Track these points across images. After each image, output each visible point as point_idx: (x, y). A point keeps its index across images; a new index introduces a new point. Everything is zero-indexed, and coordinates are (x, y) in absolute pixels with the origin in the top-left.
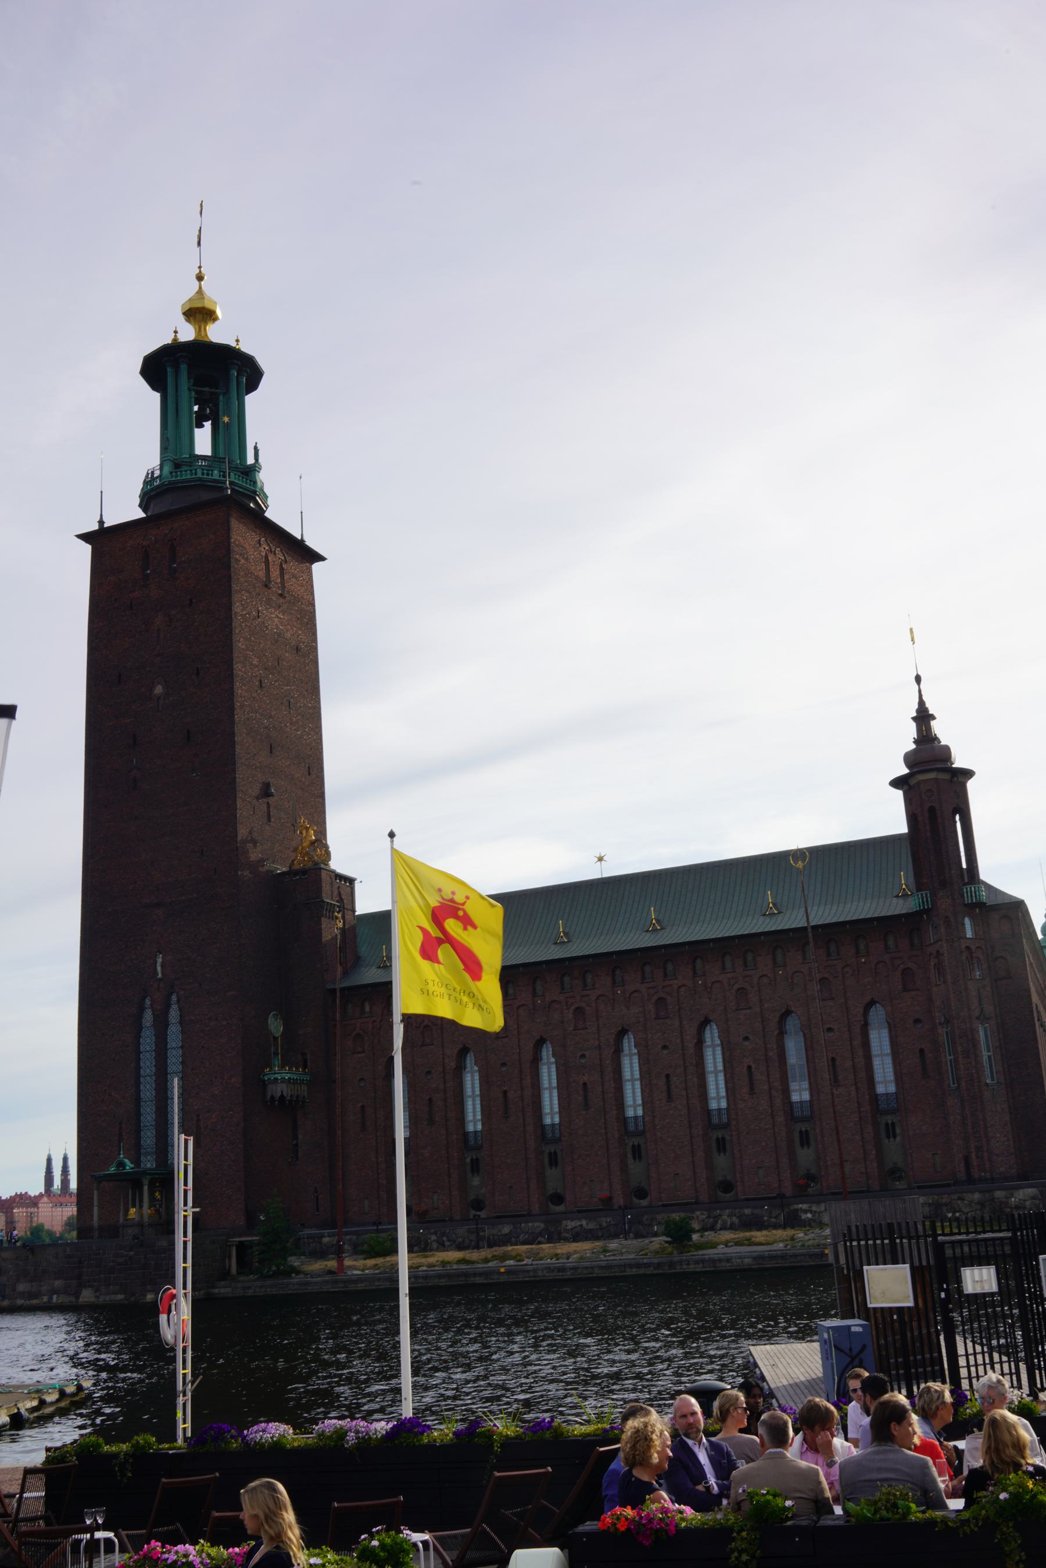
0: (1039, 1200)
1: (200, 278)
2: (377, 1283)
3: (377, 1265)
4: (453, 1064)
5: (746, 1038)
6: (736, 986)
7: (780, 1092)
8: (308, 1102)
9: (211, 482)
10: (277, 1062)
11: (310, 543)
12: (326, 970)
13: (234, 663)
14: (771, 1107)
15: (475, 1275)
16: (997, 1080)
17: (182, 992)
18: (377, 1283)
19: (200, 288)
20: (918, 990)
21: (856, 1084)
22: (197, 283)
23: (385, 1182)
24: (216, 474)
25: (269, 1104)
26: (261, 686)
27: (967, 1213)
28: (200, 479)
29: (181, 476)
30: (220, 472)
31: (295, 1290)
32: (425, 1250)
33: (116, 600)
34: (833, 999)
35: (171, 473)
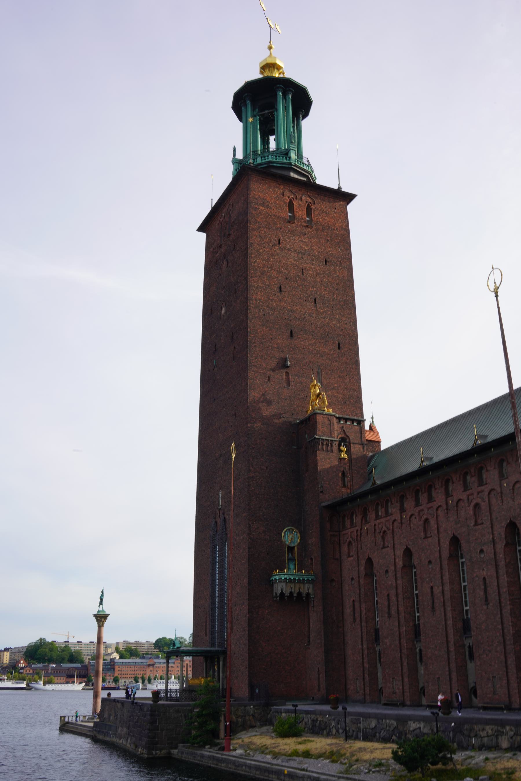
1: (270, 48)
8: (314, 598)
12: (322, 492)
13: (249, 277)
22: (268, 51)
26: (280, 290)
30: (262, 158)
31: (199, 760)
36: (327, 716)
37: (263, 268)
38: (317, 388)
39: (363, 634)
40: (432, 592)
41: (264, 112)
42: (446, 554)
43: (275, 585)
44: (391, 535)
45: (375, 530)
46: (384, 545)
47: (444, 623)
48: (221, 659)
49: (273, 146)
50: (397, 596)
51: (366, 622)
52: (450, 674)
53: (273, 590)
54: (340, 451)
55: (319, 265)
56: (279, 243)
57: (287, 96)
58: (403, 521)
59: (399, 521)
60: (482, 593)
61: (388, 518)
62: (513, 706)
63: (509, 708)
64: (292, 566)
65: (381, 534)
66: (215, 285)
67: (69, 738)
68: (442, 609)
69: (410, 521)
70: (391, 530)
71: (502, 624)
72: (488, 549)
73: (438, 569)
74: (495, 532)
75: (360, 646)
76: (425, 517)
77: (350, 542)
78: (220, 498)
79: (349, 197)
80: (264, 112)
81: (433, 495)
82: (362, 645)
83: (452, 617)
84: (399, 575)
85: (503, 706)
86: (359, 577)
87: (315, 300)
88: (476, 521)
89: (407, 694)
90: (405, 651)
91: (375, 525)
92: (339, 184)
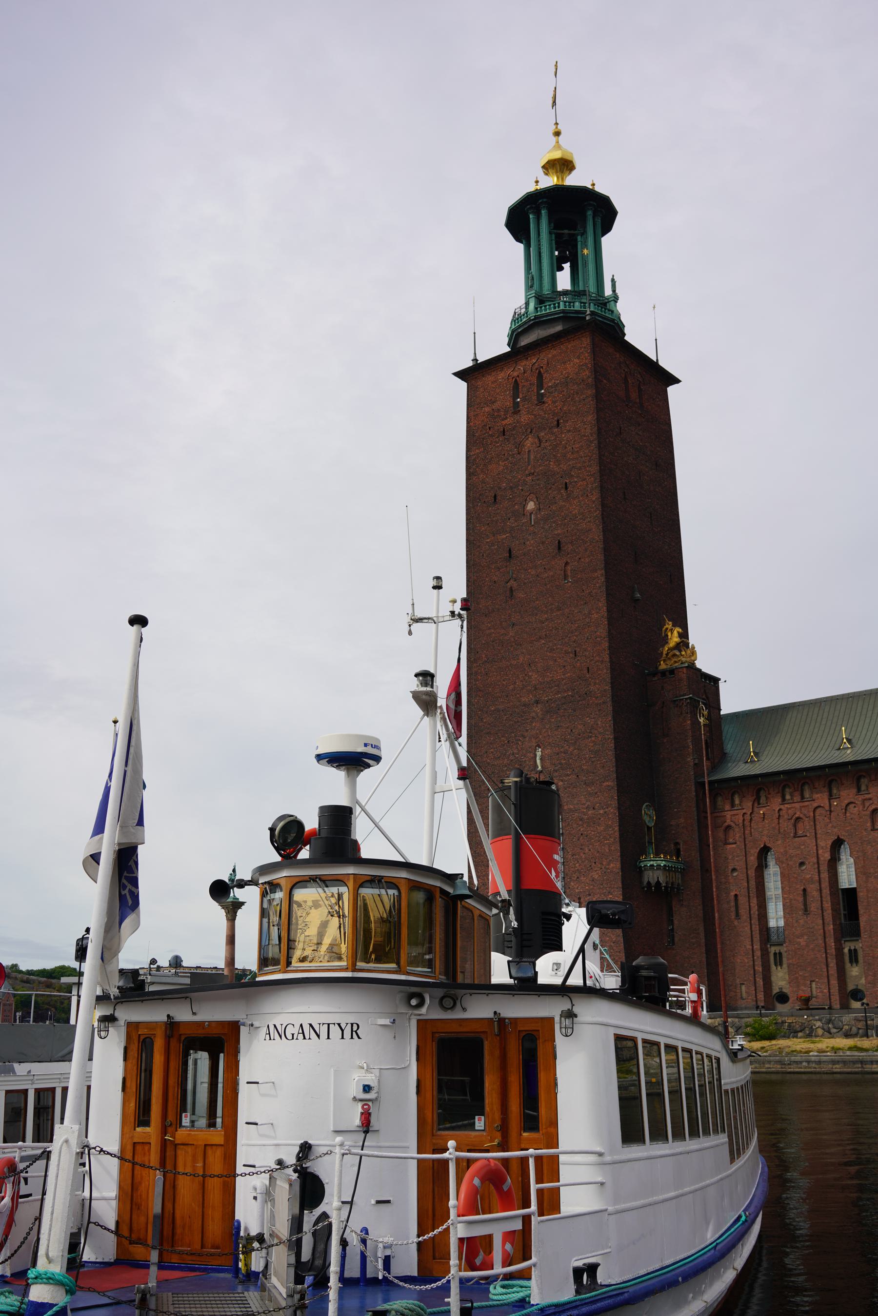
1: (557, 134)
2: (767, 1066)
3: (764, 1047)
4: (827, 856)
8: (682, 890)
9: (572, 313)
10: (651, 850)
15: (872, 1062)
17: (560, 783)
18: (767, 1066)
22: (554, 139)
23: (760, 969)
24: (577, 306)
25: (646, 889)
28: (563, 311)
29: (546, 310)
30: (581, 303)
32: (809, 1035)
33: (490, 428)
35: (536, 308)
36: (805, 1017)
38: (675, 633)
39: (754, 933)
41: (563, 232)
44: (812, 823)
46: (796, 833)
57: (596, 220)
58: (832, 809)
59: (827, 808)
61: (807, 803)
65: (793, 821)
69: (846, 809)
70: (812, 817)
78: (538, 758)
80: (563, 232)
90: (832, 951)
91: (780, 810)
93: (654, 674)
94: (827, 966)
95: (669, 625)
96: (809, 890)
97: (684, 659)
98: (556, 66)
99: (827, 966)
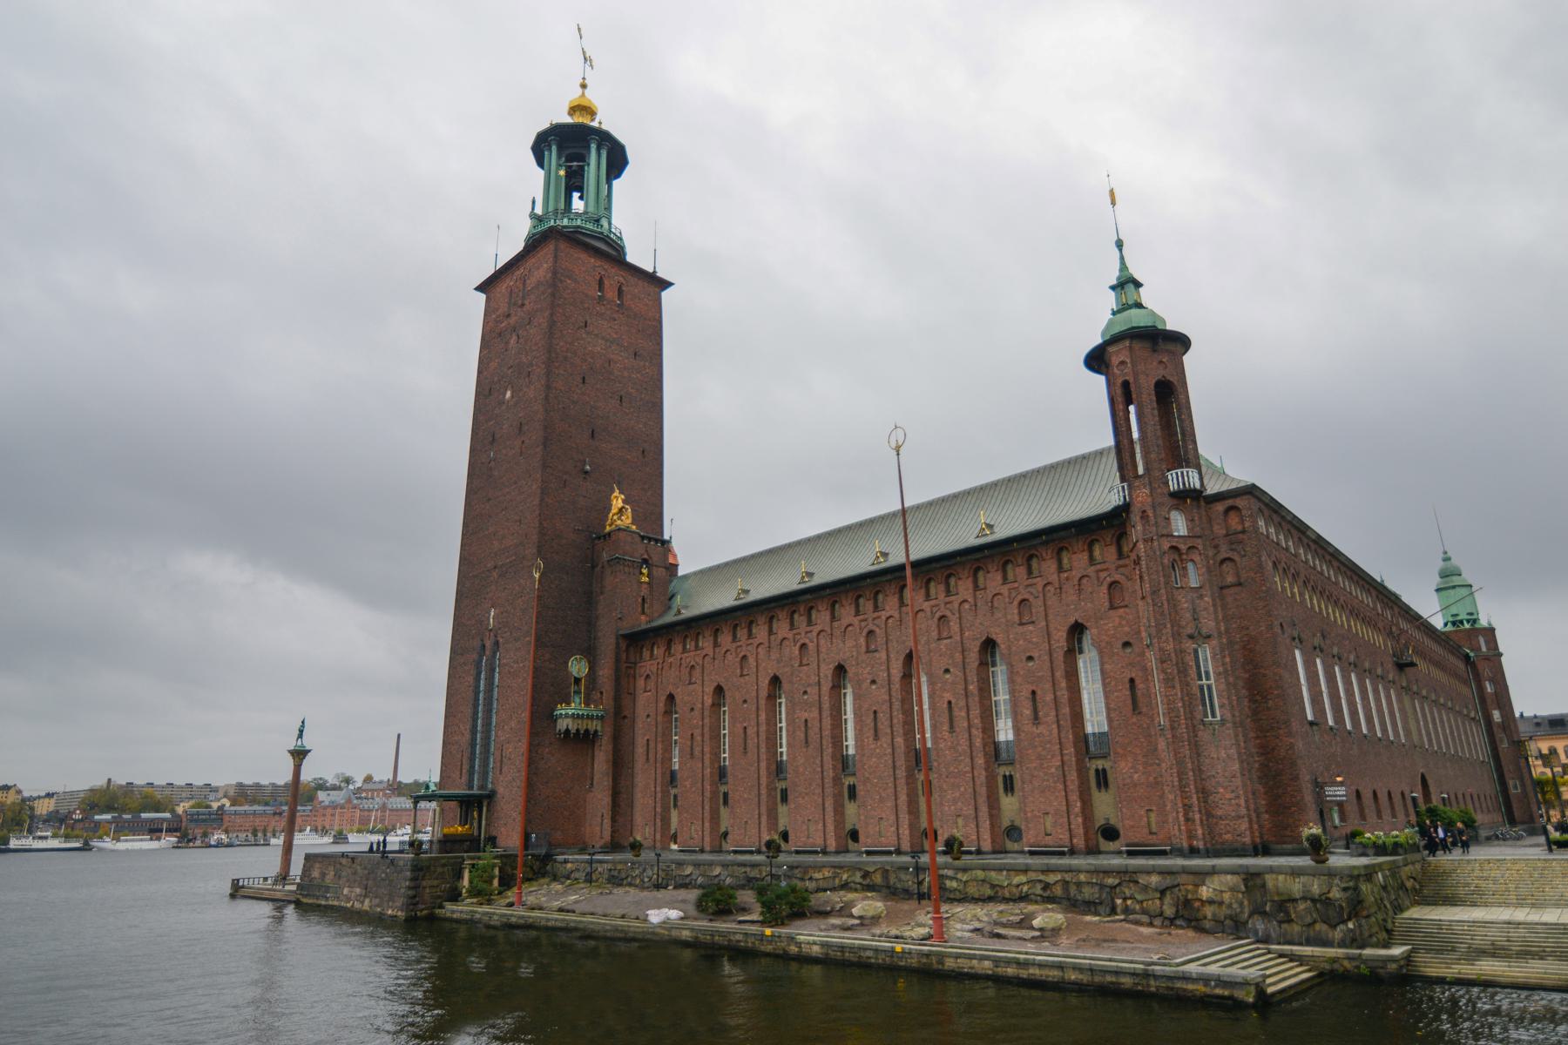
0: (1243, 893)
1: (584, 86)
5: (947, 671)
6: (938, 615)
7: (980, 730)
11: (660, 274)
12: (620, 618)
14: (971, 747)
16: (1221, 716)
19: (583, 93)
20: (1126, 606)
21: (1058, 721)
22: (580, 91)
26: (584, 382)
27: (1142, 902)
34: (1033, 622)
37: (567, 352)
38: (620, 501)
40: (745, 732)
42: (764, 693)
43: (560, 721)
45: (681, 664)
47: (756, 764)
48: (485, 804)
49: (578, 205)
50: (703, 735)
51: (662, 763)
52: (759, 818)
53: (556, 727)
54: (641, 573)
55: (627, 358)
56: (586, 326)
60: (802, 735)
61: (699, 652)
62: (828, 850)
63: (824, 852)
64: (577, 700)
65: (688, 669)
66: (497, 361)
67: (243, 905)
68: (756, 750)
71: (822, 766)
72: (813, 691)
73: (754, 708)
74: (821, 674)
75: (653, 789)
76: (742, 654)
77: (648, 676)
78: (491, 616)
79: (665, 284)
81: (754, 631)
82: (655, 787)
83: (767, 759)
84: (707, 713)
85: (819, 849)
86: (656, 714)
87: (621, 397)
88: (801, 662)
89: (707, 839)
90: (707, 794)
91: (681, 659)
92: (655, 268)
93: (599, 538)
94: (703, 808)
95: (616, 493)
96: (695, 734)
97: (619, 522)
98: (579, 29)
99: (703, 808)
